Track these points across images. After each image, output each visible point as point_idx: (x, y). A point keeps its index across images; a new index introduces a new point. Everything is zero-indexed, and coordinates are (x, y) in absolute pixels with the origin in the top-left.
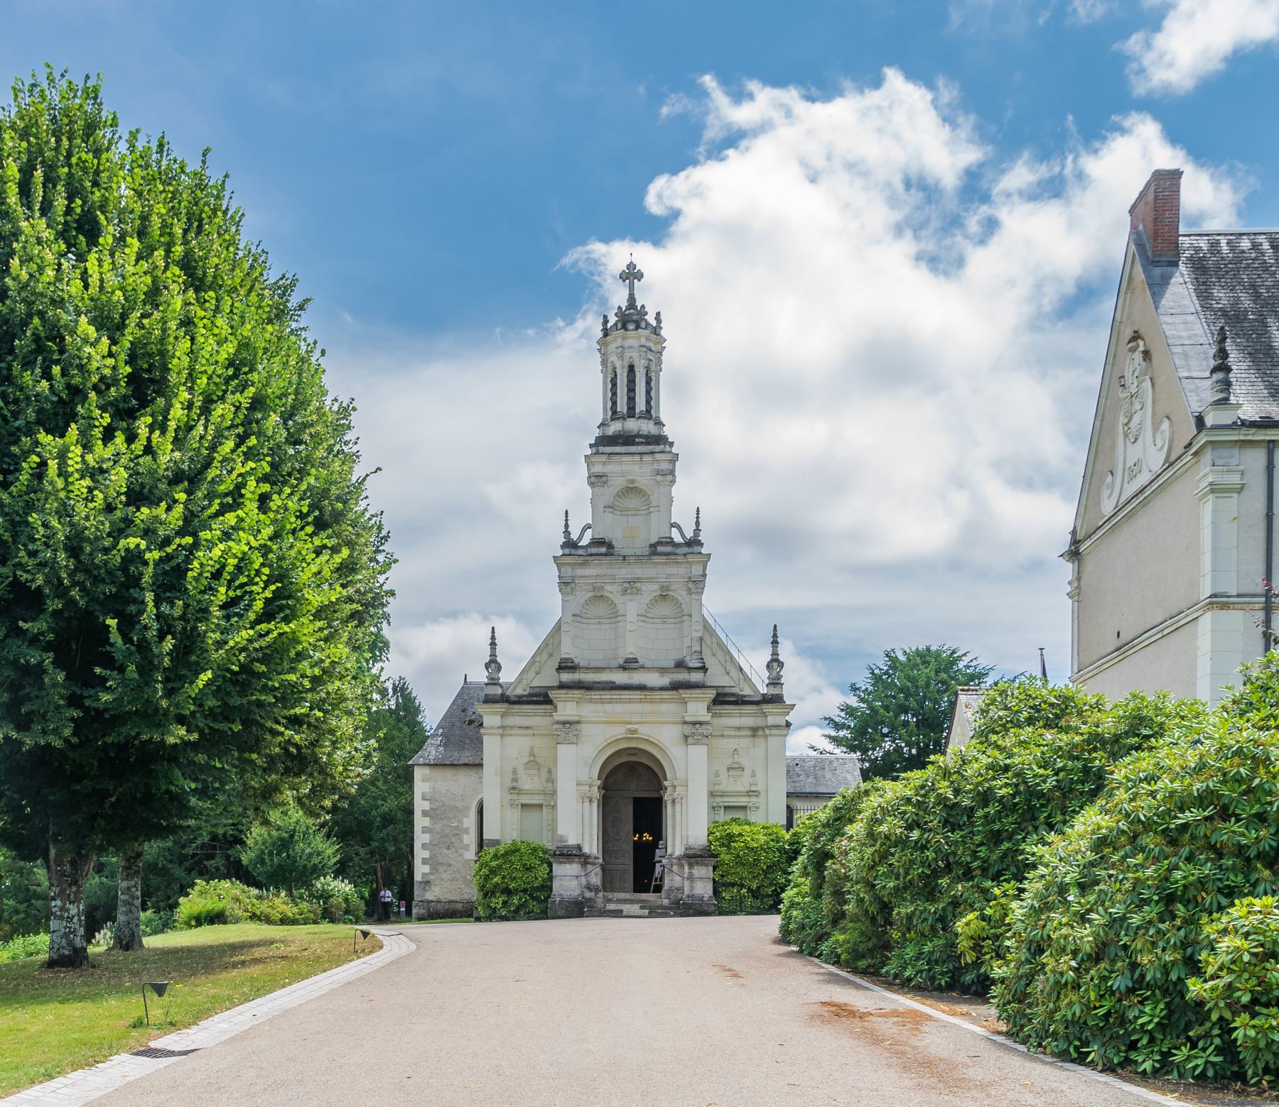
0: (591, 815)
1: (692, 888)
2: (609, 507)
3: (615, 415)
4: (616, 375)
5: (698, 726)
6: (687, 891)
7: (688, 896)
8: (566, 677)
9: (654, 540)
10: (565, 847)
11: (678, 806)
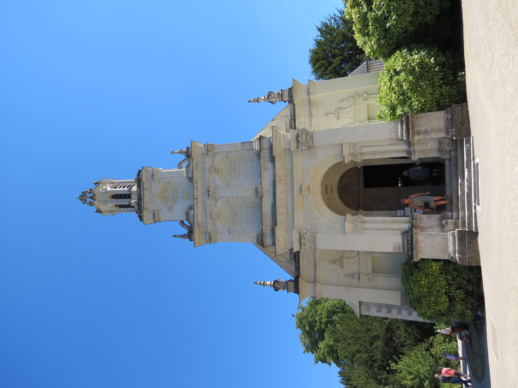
0: (375, 222)
1: (439, 130)
2: (170, 209)
3: (129, 206)
4: (116, 205)
5: (299, 139)
6: (442, 135)
7: (448, 132)
8: (268, 241)
9: (187, 180)
10: (403, 246)
11: (364, 150)
